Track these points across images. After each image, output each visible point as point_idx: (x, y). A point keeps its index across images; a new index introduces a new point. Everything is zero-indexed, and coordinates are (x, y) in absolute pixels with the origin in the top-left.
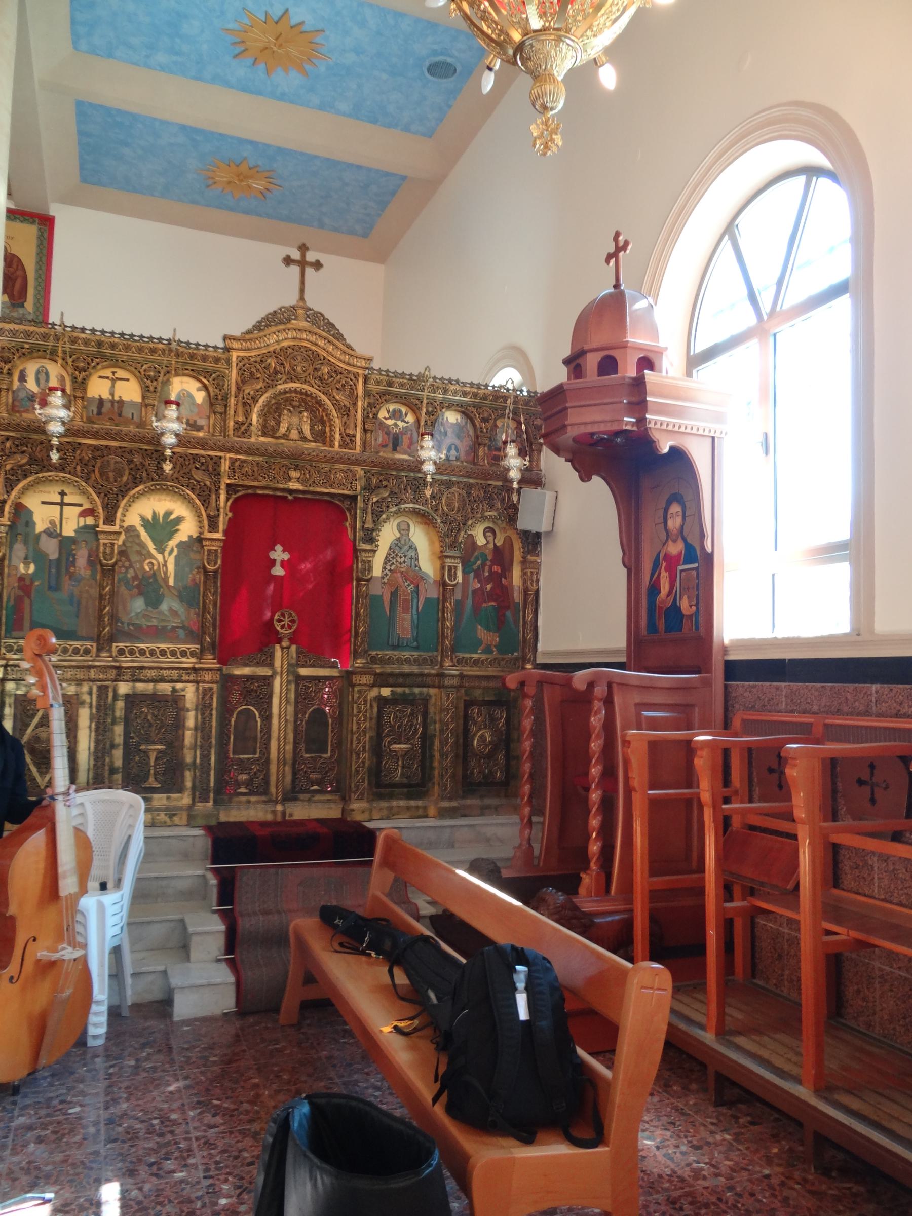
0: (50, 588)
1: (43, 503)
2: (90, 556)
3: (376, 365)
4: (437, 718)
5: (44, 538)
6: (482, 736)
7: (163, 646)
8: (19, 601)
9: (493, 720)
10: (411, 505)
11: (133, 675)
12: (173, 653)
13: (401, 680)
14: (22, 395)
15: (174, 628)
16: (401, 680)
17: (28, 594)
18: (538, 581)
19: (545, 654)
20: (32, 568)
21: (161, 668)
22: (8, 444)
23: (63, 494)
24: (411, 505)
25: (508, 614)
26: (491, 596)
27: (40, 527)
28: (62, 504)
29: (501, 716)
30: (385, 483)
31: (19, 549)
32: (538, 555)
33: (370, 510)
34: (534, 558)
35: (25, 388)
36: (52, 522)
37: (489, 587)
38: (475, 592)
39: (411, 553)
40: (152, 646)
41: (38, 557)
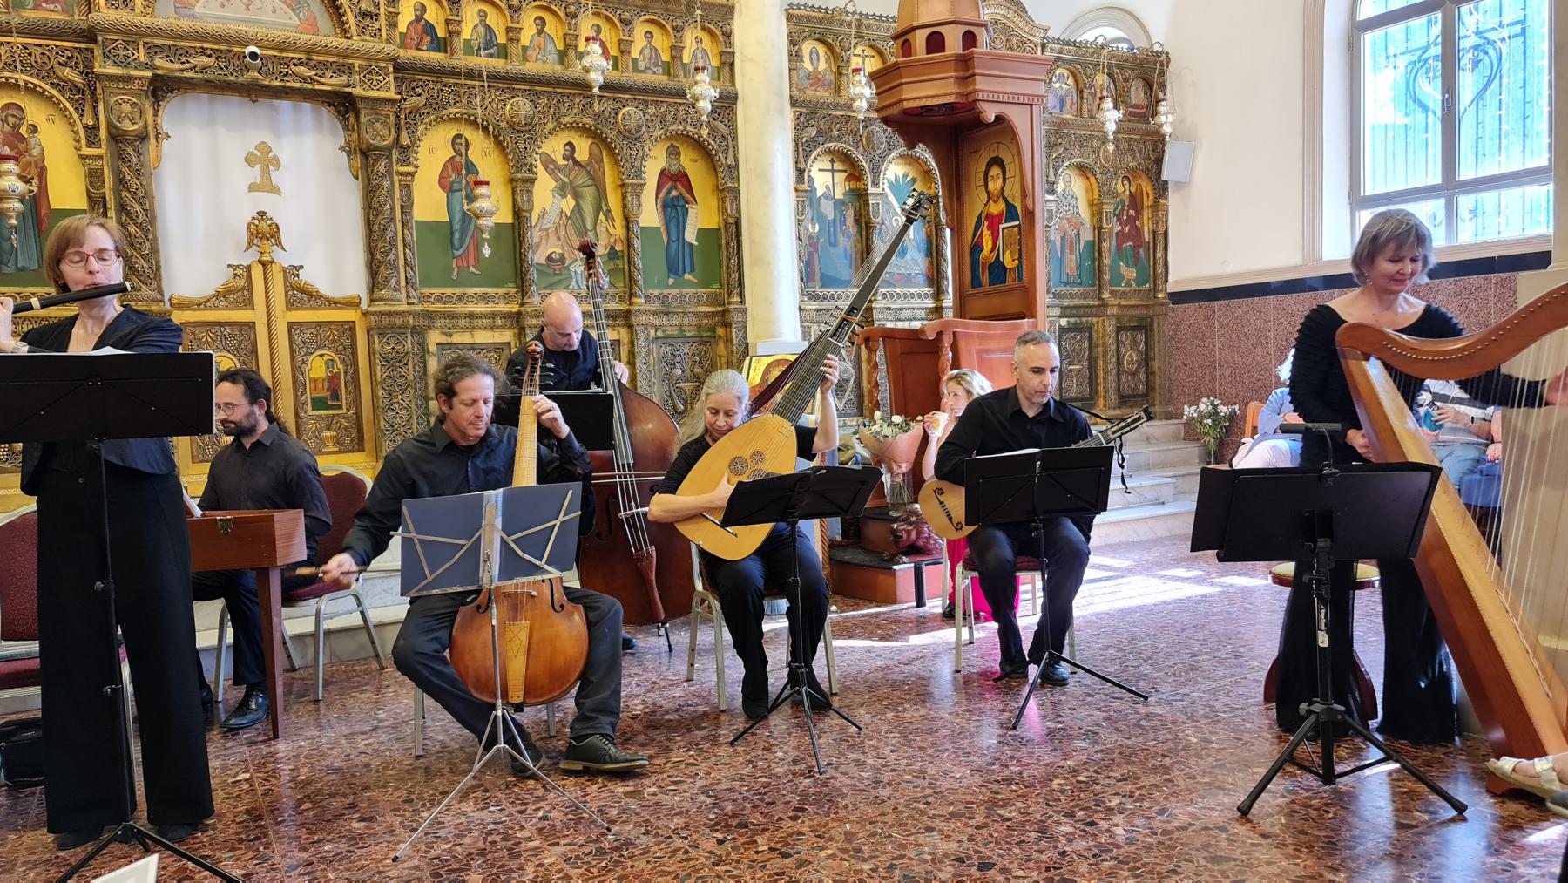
0: (830, 244)
1: (820, 170)
2: (855, 216)
3: (1050, 34)
4: (1100, 342)
5: (823, 199)
6: (1131, 356)
7: (912, 290)
8: (810, 255)
9: (1136, 343)
10: (1079, 160)
11: (895, 315)
12: (920, 296)
13: (1074, 312)
14: (802, 74)
15: (917, 274)
16: (1074, 312)
17: (817, 251)
18: (1167, 221)
19: (1175, 282)
20: (817, 226)
21: (914, 309)
22: (802, 119)
23: (832, 161)
24: (1079, 160)
25: (1141, 251)
26: (1130, 237)
27: (819, 192)
28: (833, 171)
29: (1141, 337)
30: (1060, 141)
31: (808, 212)
32: (1166, 199)
33: (1051, 165)
34: (1164, 202)
35: (803, 68)
36: (827, 187)
37: (1127, 229)
38: (1117, 233)
39: (1073, 202)
40: (905, 290)
41: (820, 218)
